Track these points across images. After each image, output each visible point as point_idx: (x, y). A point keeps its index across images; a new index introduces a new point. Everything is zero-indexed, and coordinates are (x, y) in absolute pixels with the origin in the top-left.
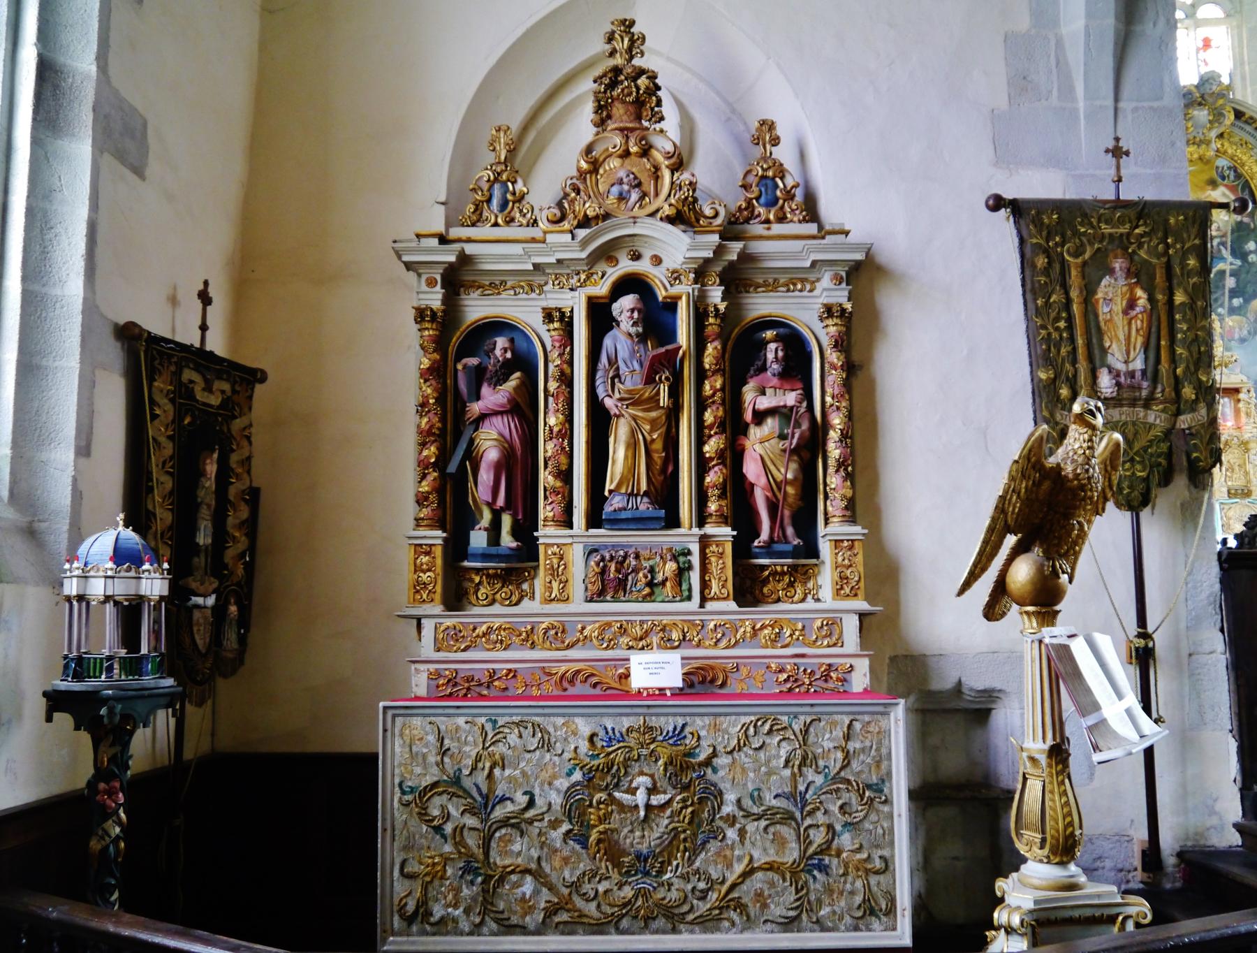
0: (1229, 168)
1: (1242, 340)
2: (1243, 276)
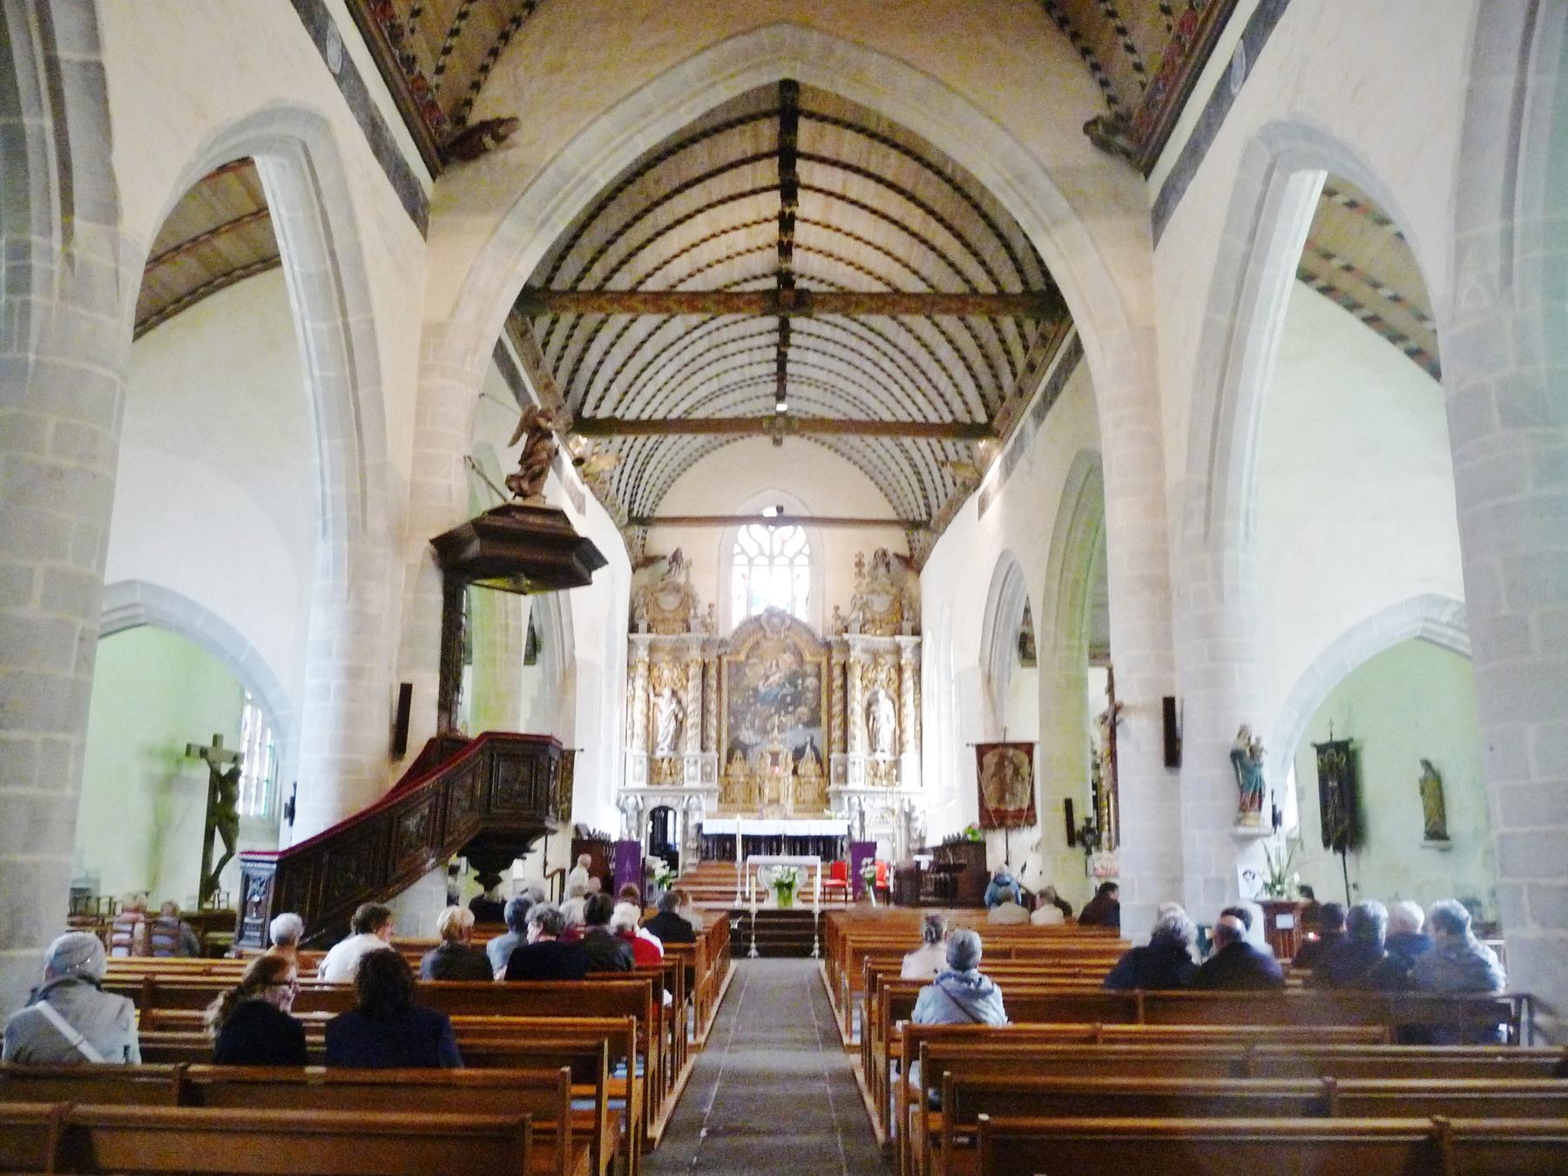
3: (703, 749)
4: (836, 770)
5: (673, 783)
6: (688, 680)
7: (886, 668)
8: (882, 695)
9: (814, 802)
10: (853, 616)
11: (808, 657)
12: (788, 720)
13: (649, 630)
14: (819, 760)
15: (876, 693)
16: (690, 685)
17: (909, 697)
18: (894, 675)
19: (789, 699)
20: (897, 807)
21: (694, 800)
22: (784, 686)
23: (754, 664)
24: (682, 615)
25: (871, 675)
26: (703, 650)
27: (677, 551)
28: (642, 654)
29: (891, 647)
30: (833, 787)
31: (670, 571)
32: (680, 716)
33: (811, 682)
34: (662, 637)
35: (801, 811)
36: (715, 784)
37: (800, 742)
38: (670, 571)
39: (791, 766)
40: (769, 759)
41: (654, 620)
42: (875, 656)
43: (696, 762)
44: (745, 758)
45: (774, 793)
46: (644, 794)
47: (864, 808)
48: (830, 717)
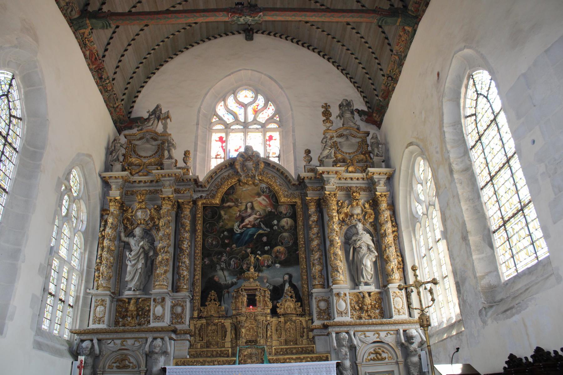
0: (266, 188)
1: (268, 266)
3: (176, 288)
4: (318, 307)
5: (139, 324)
7: (361, 202)
8: (360, 226)
11: (283, 200)
12: (265, 259)
14: (299, 299)
15: (355, 226)
17: (388, 227)
18: (370, 211)
19: (265, 239)
20: (390, 339)
21: (159, 342)
22: (258, 227)
23: (230, 207)
25: (345, 210)
26: (177, 191)
27: (158, 107)
28: (115, 193)
29: (361, 184)
30: (317, 323)
32: (151, 253)
33: (286, 222)
34: (137, 178)
37: (279, 280)
39: (270, 305)
42: (349, 193)
43: (163, 299)
44: (220, 301)
46: (100, 337)
47: (355, 343)
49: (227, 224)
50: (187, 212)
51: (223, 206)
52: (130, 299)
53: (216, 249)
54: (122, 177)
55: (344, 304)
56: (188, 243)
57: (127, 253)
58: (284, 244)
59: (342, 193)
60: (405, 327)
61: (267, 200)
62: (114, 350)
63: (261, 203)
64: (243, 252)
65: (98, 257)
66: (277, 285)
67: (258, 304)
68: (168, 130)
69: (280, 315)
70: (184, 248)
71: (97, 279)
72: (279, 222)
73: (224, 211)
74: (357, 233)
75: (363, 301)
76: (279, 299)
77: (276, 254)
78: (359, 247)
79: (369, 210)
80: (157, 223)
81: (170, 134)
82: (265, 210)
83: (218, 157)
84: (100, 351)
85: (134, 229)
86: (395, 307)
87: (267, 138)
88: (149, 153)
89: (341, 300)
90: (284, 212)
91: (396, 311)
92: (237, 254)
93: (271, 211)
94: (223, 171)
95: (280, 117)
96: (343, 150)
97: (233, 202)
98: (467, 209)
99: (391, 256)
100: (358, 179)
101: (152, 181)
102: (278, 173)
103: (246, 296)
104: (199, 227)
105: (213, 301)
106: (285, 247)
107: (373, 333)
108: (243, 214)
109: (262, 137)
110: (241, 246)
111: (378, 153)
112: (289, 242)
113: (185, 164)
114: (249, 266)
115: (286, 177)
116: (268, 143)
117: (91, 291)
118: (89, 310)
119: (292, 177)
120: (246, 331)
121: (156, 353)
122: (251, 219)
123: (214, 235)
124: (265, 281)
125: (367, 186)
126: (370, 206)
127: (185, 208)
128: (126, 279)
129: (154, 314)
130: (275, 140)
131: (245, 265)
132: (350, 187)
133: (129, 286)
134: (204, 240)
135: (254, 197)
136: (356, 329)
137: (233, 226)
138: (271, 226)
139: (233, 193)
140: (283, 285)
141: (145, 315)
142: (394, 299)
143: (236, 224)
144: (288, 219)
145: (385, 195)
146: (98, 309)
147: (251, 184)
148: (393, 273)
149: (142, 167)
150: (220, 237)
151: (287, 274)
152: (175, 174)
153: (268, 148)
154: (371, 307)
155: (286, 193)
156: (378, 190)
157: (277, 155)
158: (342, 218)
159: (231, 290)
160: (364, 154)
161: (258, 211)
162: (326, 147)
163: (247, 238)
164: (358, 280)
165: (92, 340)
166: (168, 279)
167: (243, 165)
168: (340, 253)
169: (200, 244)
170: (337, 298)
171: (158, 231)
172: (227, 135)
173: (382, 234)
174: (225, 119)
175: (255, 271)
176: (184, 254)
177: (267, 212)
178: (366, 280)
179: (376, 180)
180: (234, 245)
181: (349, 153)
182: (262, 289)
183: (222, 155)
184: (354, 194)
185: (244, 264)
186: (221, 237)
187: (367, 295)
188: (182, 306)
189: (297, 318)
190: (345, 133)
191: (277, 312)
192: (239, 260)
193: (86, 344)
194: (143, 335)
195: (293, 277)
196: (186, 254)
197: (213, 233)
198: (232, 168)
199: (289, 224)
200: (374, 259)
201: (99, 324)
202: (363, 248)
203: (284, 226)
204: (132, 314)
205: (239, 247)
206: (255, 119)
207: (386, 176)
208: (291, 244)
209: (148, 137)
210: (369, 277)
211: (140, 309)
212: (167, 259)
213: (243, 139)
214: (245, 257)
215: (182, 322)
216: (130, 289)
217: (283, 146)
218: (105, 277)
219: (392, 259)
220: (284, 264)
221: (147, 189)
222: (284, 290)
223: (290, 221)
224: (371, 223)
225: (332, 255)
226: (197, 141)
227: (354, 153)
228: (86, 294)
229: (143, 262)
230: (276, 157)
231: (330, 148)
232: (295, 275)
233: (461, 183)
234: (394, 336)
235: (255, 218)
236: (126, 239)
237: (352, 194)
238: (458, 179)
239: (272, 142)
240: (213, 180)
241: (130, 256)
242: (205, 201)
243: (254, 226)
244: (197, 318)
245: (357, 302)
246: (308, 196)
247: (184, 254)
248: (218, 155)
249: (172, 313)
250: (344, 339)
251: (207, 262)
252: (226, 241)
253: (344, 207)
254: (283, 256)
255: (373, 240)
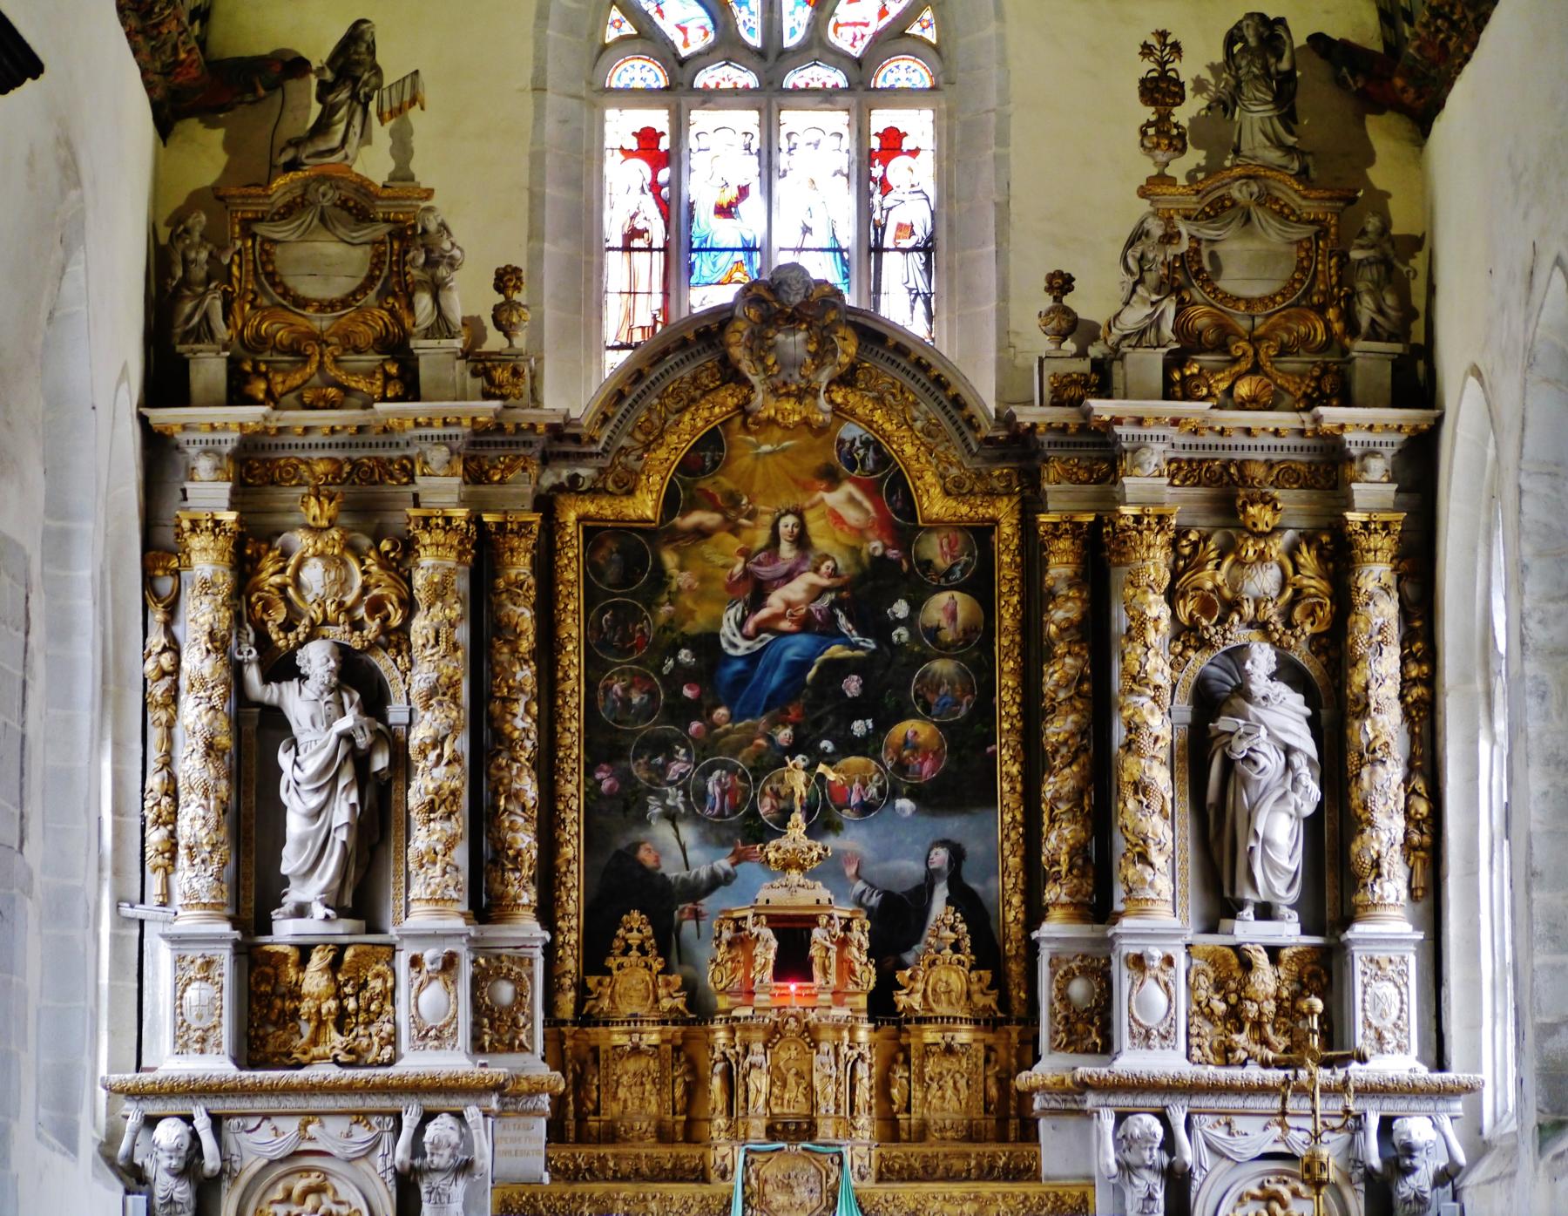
0: (866, 444)
1: (865, 808)
2: (878, 673)
4: (1064, 997)
5: (356, 1059)
6: (409, 606)
7: (1277, 546)
8: (1262, 660)
9: (972, 1134)
10: (1134, 317)
11: (934, 504)
13: (237, 394)
15: (1238, 655)
16: (421, 627)
22: (825, 630)
23: (702, 533)
24: (380, 318)
25: (1212, 577)
26: (475, 474)
29: (1288, 449)
30: (1051, 1066)
31: (323, 126)
32: (380, 761)
34: (297, 418)
35: (909, 1175)
36: (533, 1065)
37: (909, 868)
38: (323, 126)
39: (868, 976)
40: (767, 950)
41: (260, 342)
45: (794, 1092)
46: (218, 1106)
47: (1188, 1156)
48: (1035, 764)
49: (691, 614)
50: (520, 567)
51: (674, 528)
52: (305, 952)
53: (644, 727)
54: (241, 425)
55: (1160, 998)
56: (527, 711)
57: (285, 759)
58: (935, 711)
59: (1200, 491)
60: (1390, 1106)
61: (867, 504)
62: (278, 1155)
63: (838, 519)
64: (761, 742)
65: (153, 765)
66: (897, 890)
67: (817, 972)
68: (415, 166)
69: (908, 1021)
70: (516, 734)
71: (160, 860)
72: (916, 606)
73: (676, 550)
74: (1247, 696)
75: (1243, 985)
76: (908, 948)
77: (898, 752)
78: (1247, 758)
79: (1313, 582)
80: (396, 621)
81: (429, 193)
82: (855, 551)
83: (637, 243)
84: (225, 1159)
85: (301, 645)
86: (1366, 1018)
87: (875, 143)
88: (336, 288)
89: (1150, 984)
90: (941, 563)
91: (1371, 1034)
92: (735, 752)
93: (884, 556)
94: (671, 360)
95: (942, 23)
96: (1221, 284)
97: (716, 508)
98: (1546, 794)
99: (1380, 801)
100: (1276, 433)
101: (361, 429)
102: (920, 376)
103: (774, 944)
104: (572, 628)
105: (634, 953)
106: (940, 726)
107: (1263, 1121)
108: (758, 569)
109: (847, 142)
110: (752, 716)
111: (1379, 319)
112: (958, 703)
113: (505, 343)
114: (783, 804)
115: (958, 403)
116: (877, 171)
117: (139, 912)
118: (136, 985)
119: (984, 408)
120: (772, 1083)
121: (437, 1170)
122: (796, 590)
123: (637, 662)
124: (851, 871)
125: (1316, 458)
126: (1321, 557)
127: (512, 550)
128: (285, 869)
129: (416, 1018)
130: (914, 153)
131: (767, 801)
132: (1242, 465)
133: (294, 896)
134: (591, 686)
135: (807, 488)
136: (1196, 1102)
137: (718, 622)
138: (878, 627)
139: (715, 464)
140: (923, 893)
141: (368, 1010)
142: (1365, 986)
143: (732, 612)
144: (957, 595)
145: (1386, 525)
146: (192, 993)
147: (797, 424)
148: (1379, 875)
149: (312, 367)
150: (658, 672)
151: (944, 843)
152: (474, 419)
153: (877, 198)
154: (1279, 1007)
155: (954, 471)
156: (1358, 500)
157: (920, 234)
158: (1191, 616)
159: (707, 904)
160: (1321, 310)
161: (826, 557)
162: (1140, 289)
163: (776, 679)
164: (1233, 889)
165: (188, 1119)
166: (457, 869)
167: (760, 345)
168: (1160, 777)
169: (578, 707)
170: (1136, 974)
171: (399, 653)
172: (679, 126)
173: (1357, 701)
174: (667, 26)
175: (810, 833)
176: (516, 760)
177: (866, 559)
178: (1263, 896)
179: (1355, 451)
180: (722, 712)
181: (1250, 302)
182: (836, 914)
183: (658, 236)
184: (1251, 510)
185: (763, 793)
186: (665, 671)
187: (1262, 959)
188: (517, 981)
189: (980, 1036)
190: (1236, 194)
191: (895, 1005)
192: (744, 777)
193: (169, 1133)
194: (385, 1103)
195: (968, 858)
196: (523, 756)
197: (630, 651)
198: (710, 347)
199: (961, 615)
200: (1308, 810)
201: (202, 1051)
202: (1263, 761)
203: (939, 628)
204: (319, 1011)
205: (742, 718)
206: (816, 28)
207: (1403, 437)
208: (963, 711)
209: (326, 203)
210: (1280, 886)
211: (348, 990)
212: (453, 793)
213: (755, 146)
214: (771, 762)
215: (521, 1045)
216: (301, 911)
217: (950, 197)
218: (203, 861)
219: (1379, 817)
220: (933, 799)
221: (340, 455)
222: (925, 911)
223: (963, 603)
224: (1314, 637)
225: (1128, 792)
226: (542, 185)
227: (1272, 299)
228: (120, 921)
229: (354, 798)
230: (915, 249)
231: (1155, 298)
232: (974, 847)
233: (1543, 697)
234: (1343, 1137)
235: (813, 586)
236: (268, 693)
237: (1244, 505)
238: (1535, 677)
239: (898, 170)
240: (626, 405)
241: (298, 773)
242: (591, 508)
243: (806, 624)
244: (574, 1023)
245: (1219, 986)
246: (1050, 506)
247: (516, 760)
248: (635, 233)
249: (477, 1008)
250: (1148, 1141)
251: (605, 786)
252: (687, 692)
253: (1201, 566)
254: (927, 766)
255: (1313, 722)
